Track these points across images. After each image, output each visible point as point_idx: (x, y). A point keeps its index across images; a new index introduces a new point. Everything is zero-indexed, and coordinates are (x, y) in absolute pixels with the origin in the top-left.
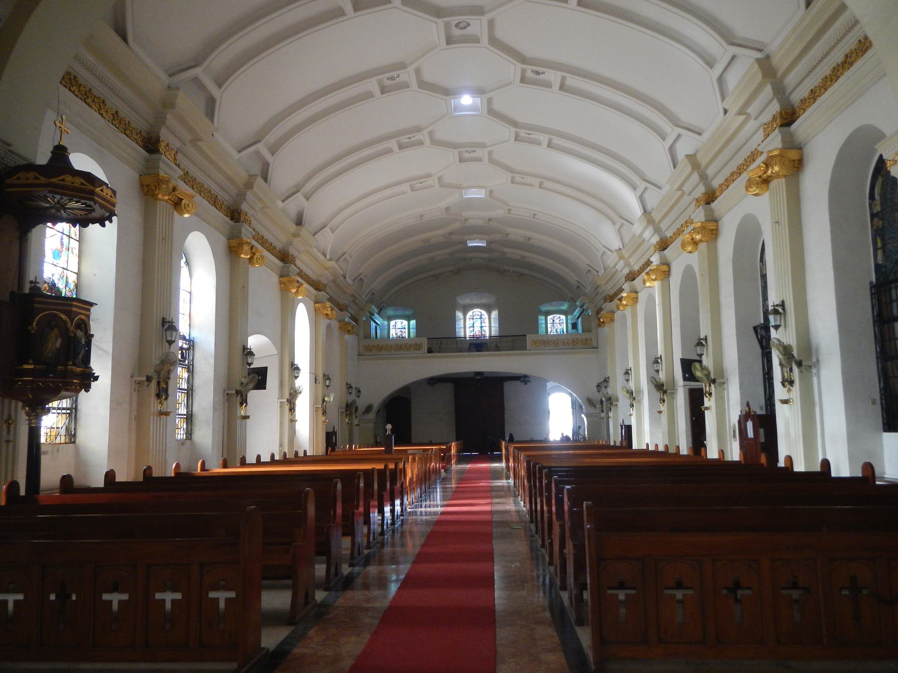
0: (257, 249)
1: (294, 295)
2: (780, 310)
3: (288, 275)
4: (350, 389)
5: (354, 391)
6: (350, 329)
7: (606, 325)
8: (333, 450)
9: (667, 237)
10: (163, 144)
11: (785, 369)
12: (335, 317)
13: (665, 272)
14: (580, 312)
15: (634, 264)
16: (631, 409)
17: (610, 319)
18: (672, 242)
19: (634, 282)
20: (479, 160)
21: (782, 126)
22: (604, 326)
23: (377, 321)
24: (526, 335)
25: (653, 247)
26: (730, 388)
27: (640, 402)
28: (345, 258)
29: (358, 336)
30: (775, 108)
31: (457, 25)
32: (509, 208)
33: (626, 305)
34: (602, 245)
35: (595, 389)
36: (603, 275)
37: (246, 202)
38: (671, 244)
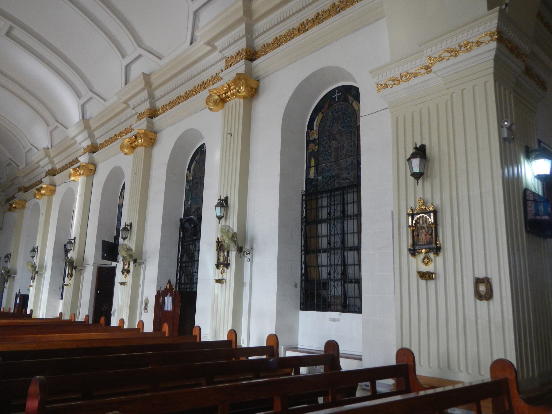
7: (17, 210)
9: (97, 143)
15: (57, 164)
16: (32, 281)
17: (21, 206)
18: (103, 148)
19: (54, 177)
25: (82, 149)
26: (147, 268)
33: (44, 194)
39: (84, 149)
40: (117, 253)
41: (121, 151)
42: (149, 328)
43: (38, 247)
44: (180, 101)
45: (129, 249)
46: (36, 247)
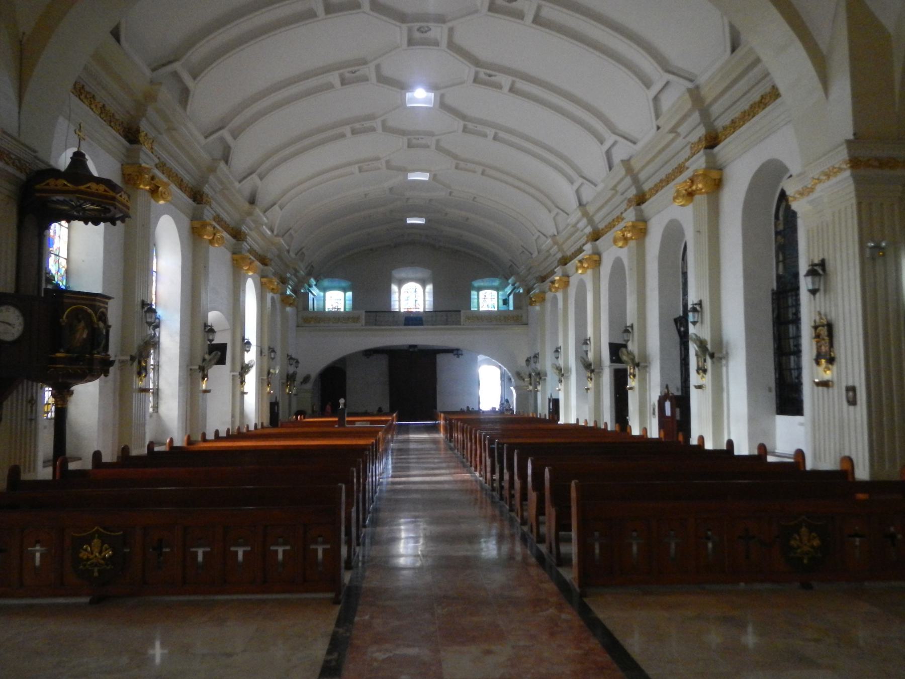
0: (218, 231)
2: (698, 308)
3: (240, 252)
5: (294, 362)
10: (143, 134)
11: (700, 359)
13: (596, 261)
19: (566, 266)
21: (707, 148)
24: (460, 311)
25: (585, 237)
27: (568, 378)
30: (701, 131)
31: (419, 30)
33: (558, 288)
35: (524, 364)
42: (654, 432)
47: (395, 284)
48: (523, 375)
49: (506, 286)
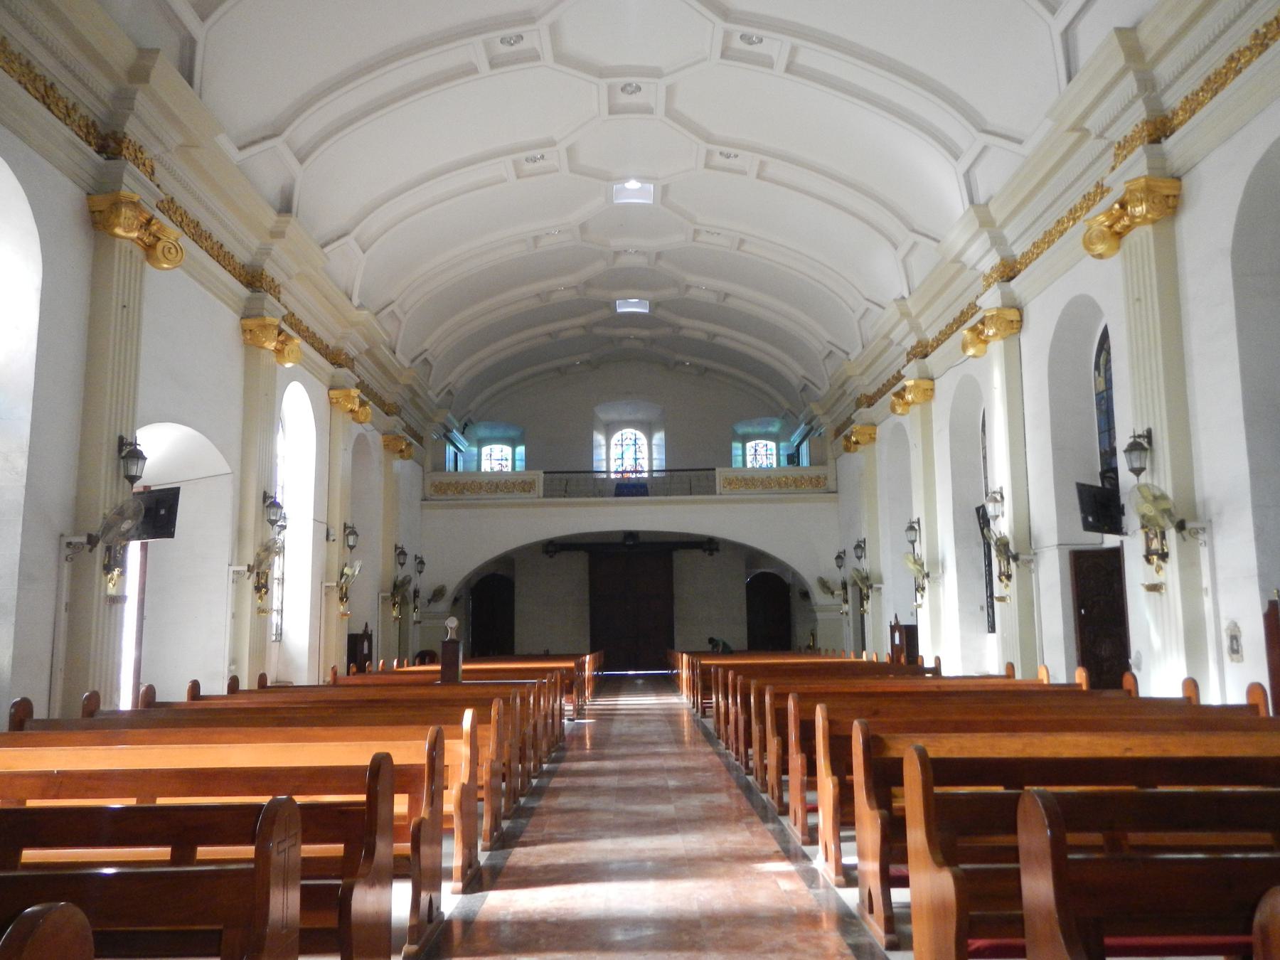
0: (162, 228)
1: (275, 359)
3: (260, 315)
4: (402, 557)
6: (403, 447)
7: (860, 448)
8: (361, 670)
9: (1014, 256)
12: (369, 419)
14: (805, 432)
15: (928, 328)
17: (868, 437)
18: (1030, 262)
19: (927, 360)
20: (648, 110)
22: (856, 450)
23: (459, 446)
24: (714, 469)
26: (1218, 541)
28: (393, 311)
29: (423, 466)
32: (697, 227)
33: (913, 402)
34: (863, 296)
35: (833, 563)
36: (857, 358)
37: (138, 117)
38: (1027, 266)
39: (986, 278)
40: (1120, 511)
41: (1086, 252)
43: (919, 519)
44: (1239, 66)
45: (1158, 498)
46: (915, 519)
47: (599, 431)
48: (831, 584)
49: (792, 433)
